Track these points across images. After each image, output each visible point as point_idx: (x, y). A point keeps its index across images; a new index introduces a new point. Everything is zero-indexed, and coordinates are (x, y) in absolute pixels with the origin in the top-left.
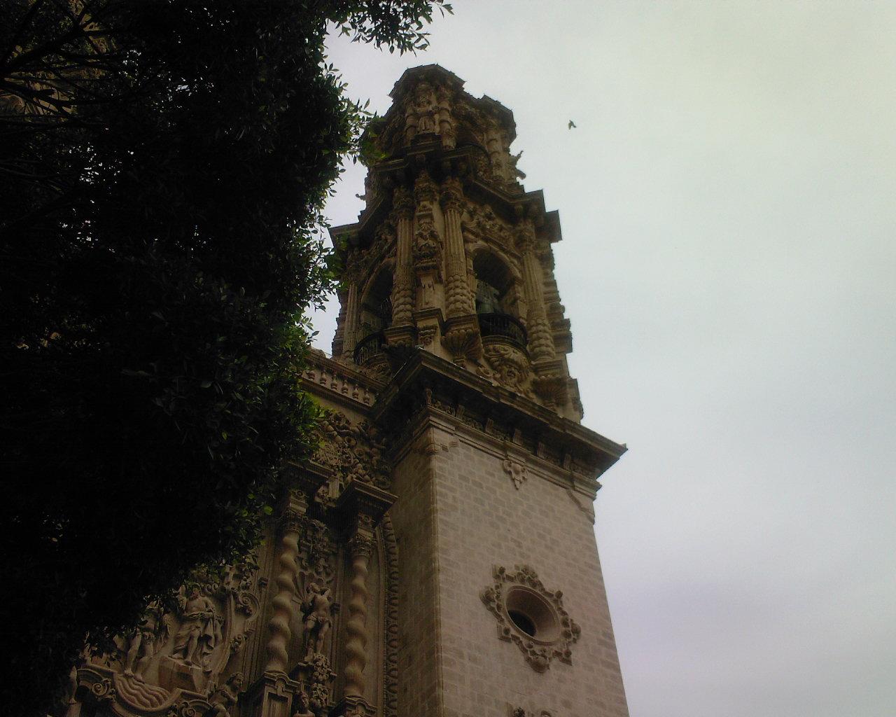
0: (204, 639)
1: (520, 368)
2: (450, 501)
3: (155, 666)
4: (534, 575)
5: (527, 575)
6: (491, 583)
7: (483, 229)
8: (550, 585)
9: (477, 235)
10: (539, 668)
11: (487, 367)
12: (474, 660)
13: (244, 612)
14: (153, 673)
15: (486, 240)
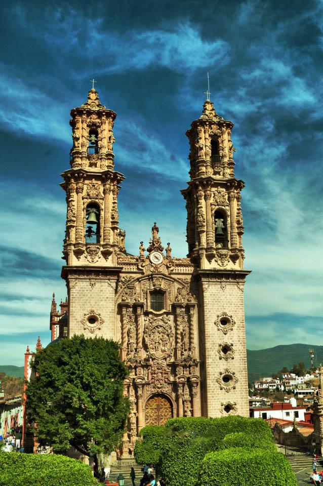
0: (166, 343)
1: (225, 255)
2: (207, 303)
3: (160, 349)
4: (226, 313)
5: (225, 314)
6: (217, 318)
7: (217, 202)
8: (229, 314)
9: (215, 206)
10: (225, 334)
11: (217, 257)
12: (212, 337)
13: (172, 337)
14: (160, 350)
15: (218, 205)
